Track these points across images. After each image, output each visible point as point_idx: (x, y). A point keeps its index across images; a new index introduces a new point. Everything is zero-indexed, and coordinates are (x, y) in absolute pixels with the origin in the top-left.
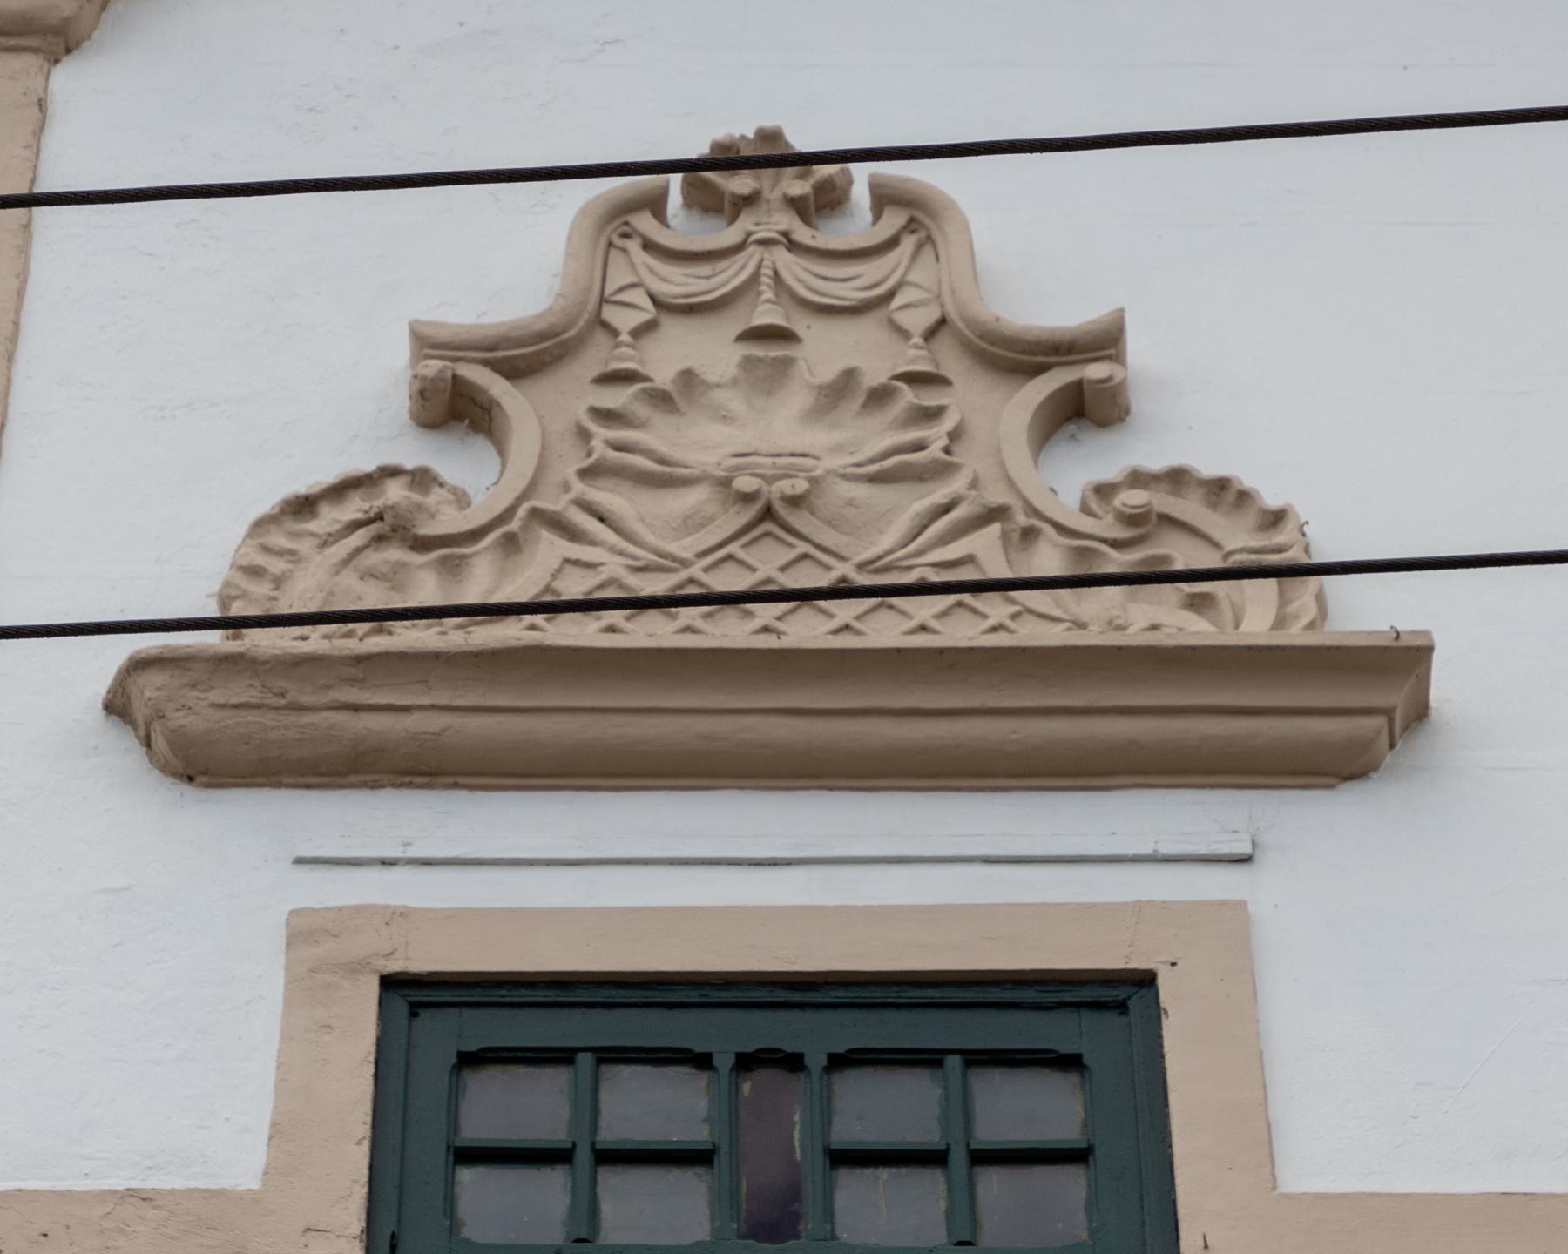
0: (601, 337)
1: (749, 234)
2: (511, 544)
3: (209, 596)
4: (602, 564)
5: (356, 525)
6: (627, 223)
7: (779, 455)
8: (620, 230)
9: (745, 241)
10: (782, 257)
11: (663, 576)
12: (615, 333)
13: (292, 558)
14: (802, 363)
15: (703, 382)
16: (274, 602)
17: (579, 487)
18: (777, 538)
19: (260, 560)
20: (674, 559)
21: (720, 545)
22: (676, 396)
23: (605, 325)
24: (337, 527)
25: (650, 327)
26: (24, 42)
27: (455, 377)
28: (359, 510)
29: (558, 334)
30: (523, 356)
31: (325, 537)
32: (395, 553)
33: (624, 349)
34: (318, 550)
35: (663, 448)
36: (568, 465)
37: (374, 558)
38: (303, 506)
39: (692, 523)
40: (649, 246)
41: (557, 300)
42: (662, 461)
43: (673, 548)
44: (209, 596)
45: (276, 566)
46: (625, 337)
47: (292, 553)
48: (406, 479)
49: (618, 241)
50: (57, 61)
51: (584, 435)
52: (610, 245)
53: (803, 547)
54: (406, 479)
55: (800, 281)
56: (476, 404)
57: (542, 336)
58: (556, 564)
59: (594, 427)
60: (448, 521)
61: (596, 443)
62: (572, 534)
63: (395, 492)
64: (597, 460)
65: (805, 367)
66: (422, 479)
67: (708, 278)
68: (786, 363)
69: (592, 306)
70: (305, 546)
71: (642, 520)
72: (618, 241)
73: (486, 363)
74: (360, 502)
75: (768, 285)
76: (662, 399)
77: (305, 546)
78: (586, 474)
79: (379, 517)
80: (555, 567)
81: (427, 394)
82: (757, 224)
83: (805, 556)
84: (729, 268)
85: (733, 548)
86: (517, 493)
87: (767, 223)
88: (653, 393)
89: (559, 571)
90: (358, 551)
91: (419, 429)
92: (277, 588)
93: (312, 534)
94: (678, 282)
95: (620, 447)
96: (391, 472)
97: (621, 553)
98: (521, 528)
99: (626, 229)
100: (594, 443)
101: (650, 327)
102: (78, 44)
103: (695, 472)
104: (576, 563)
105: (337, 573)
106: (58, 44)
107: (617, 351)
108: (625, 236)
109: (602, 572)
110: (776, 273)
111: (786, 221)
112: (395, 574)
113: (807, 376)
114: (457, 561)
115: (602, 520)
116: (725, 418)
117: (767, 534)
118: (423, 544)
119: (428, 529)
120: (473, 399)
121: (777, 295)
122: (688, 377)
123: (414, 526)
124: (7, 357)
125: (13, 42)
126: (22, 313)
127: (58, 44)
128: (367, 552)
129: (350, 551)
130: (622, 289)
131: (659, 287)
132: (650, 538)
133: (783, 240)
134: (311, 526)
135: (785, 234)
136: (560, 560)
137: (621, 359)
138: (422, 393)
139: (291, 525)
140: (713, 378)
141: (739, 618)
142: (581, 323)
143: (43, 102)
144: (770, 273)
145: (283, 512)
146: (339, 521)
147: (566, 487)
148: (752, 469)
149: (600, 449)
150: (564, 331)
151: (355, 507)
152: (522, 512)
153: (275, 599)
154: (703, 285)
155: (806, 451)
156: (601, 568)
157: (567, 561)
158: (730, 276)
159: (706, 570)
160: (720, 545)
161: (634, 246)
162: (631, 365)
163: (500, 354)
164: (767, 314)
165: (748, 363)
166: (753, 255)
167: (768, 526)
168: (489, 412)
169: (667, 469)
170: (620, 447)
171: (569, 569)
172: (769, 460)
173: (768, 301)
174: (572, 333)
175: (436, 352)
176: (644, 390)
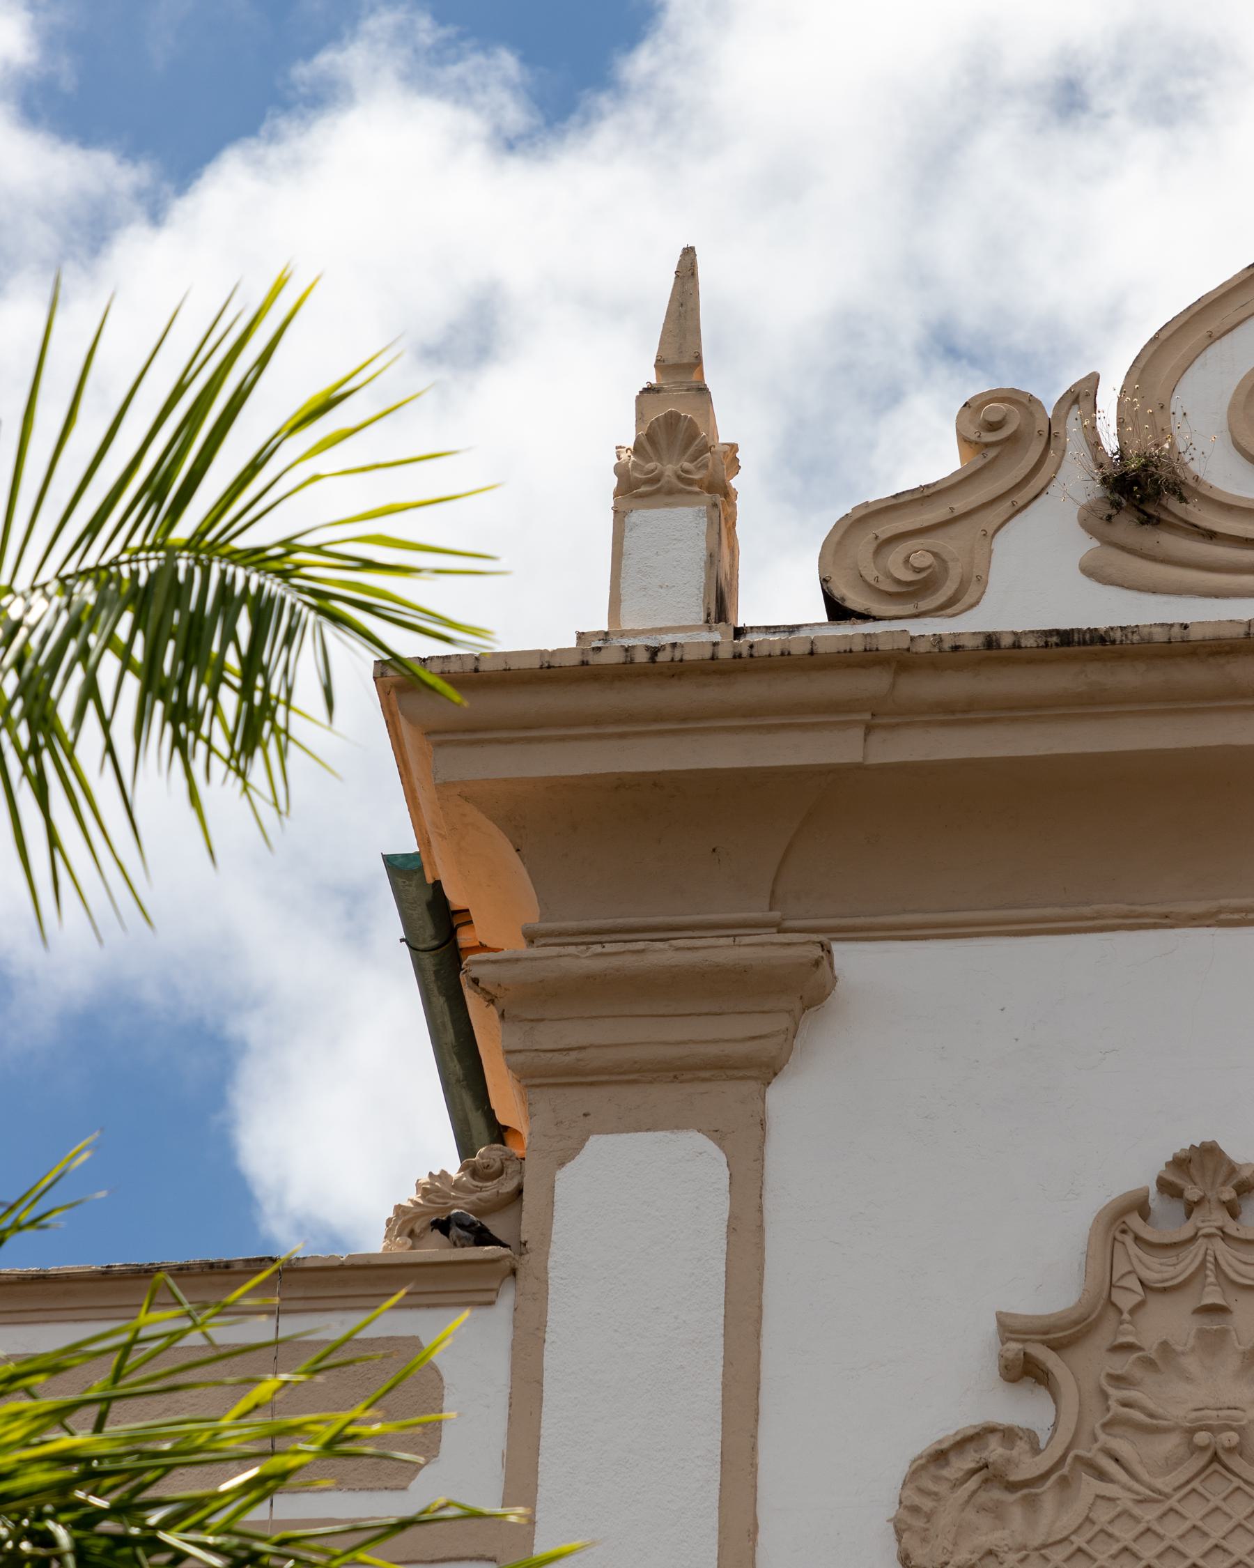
0: (1112, 1314)
1: (1199, 1229)
2: (1064, 1482)
3: (888, 1521)
4: (1118, 1499)
5: (974, 1472)
6: (1124, 1222)
7: (1221, 1409)
8: (1120, 1228)
9: (1196, 1234)
10: (1219, 1246)
11: (1156, 1506)
12: (1120, 1312)
13: (936, 1498)
14: (1233, 1333)
15: (1174, 1350)
16: (927, 1532)
17: (1102, 1437)
18: (1221, 1474)
19: (918, 1500)
20: (1160, 1493)
21: (1188, 1482)
22: (1157, 1361)
23: (1114, 1305)
24: (961, 1474)
25: (1141, 1305)
26: (749, 1073)
27: (1025, 1354)
28: (974, 1460)
29: (1085, 1319)
30: (1065, 1336)
31: (954, 1482)
32: (997, 1494)
33: (1126, 1326)
34: (950, 1491)
35: (1151, 1405)
36: (1095, 1421)
37: (983, 1497)
38: (940, 1456)
39: (1171, 1465)
40: (1138, 1239)
41: (1083, 1294)
42: (1151, 1416)
43: (1159, 1483)
44: (888, 1521)
45: (927, 1504)
46: (1126, 1316)
47: (936, 1494)
48: (999, 1435)
49: (1119, 1236)
50: (769, 1083)
51: (1105, 1396)
52: (1115, 1239)
53: (1237, 1482)
54: (999, 1435)
55: (1230, 1266)
56: (1039, 1368)
57: (1076, 1323)
58: (1091, 1499)
59: (1111, 1391)
60: (1028, 1468)
61: (1112, 1403)
62: (1102, 1475)
63: (995, 1450)
64: (1113, 1416)
65: (1235, 1338)
66: (1009, 1435)
67: (1174, 1265)
68: (1224, 1333)
69: (1105, 1294)
70: (942, 1488)
71: (1141, 1462)
72: (1119, 1236)
73: (1043, 1342)
74: (973, 1453)
75: (1211, 1270)
76: (1149, 1363)
77: (942, 1488)
78: (1105, 1426)
79: (986, 1466)
80: (1091, 1502)
81: (1009, 1367)
82: (1203, 1221)
83: (1238, 1488)
84: (1187, 1257)
85: (1195, 1484)
86: (1065, 1445)
87: (1209, 1221)
88: (1145, 1360)
89: (1093, 1504)
90: (974, 1492)
91: (1006, 1383)
92: (928, 1521)
93: (947, 1479)
94: (1158, 1269)
95: (1126, 1404)
96: (990, 1430)
97: (1130, 1490)
98: (1069, 1471)
99: (1123, 1226)
100: (1110, 1403)
101: (1141, 1305)
102: (781, 1069)
103: (1171, 1423)
104: (1103, 1497)
105: (963, 1510)
106: (769, 1073)
107: (1122, 1327)
108: (1124, 1232)
109: (1118, 1505)
110: (1216, 1259)
111: (1220, 1218)
112: (997, 1508)
113: (1236, 1344)
114: (1033, 1498)
115: (1117, 1460)
116: (1188, 1379)
117: (1216, 1471)
118: (1012, 1487)
119: (1016, 1476)
120: (1037, 1366)
121: (1217, 1277)
122: (1165, 1346)
123: (1006, 1475)
124: (756, 1335)
125: (741, 1073)
126: (764, 1297)
127: (769, 1073)
128: (981, 1493)
129: (970, 1493)
130: (1123, 1276)
131: (1148, 1275)
132: (1146, 1477)
133: (1220, 1234)
134: (945, 1472)
135: (1221, 1229)
136: (1093, 1497)
137: (1124, 1334)
138: (1006, 1367)
139: (932, 1469)
140: (1179, 1348)
141: (1200, 1537)
142: (1099, 1308)
143: (764, 1122)
144: (1212, 1259)
145: (928, 1462)
146: (962, 1470)
147: (1096, 1440)
148: (1205, 1420)
149: (1116, 1409)
150: (1089, 1316)
151: (967, 1461)
152: (1069, 1460)
153: (927, 1530)
154: (1170, 1272)
155: (1238, 1405)
156: (1118, 1502)
157: (1098, 1496)
158: (1188, 1262)
159: (1179, 1501)
160: (1188, 1482)
161: (1128, 1239)
162: (1130, 1339)
163: (1051, 1336)
164: (1212, 1297)
165: (1202, 1333)
166: (1201, 1244)
167: (1216, 1466)
168: (1047, 1374)
169: (1155, 1422)
170: (1126, 1404)
171: (1099, 1502)
172: (1214, 1413)
173: (1211, 1284)
174: (1094, 1316)
175: (1013, 1336)
176: (1139, 1358)
